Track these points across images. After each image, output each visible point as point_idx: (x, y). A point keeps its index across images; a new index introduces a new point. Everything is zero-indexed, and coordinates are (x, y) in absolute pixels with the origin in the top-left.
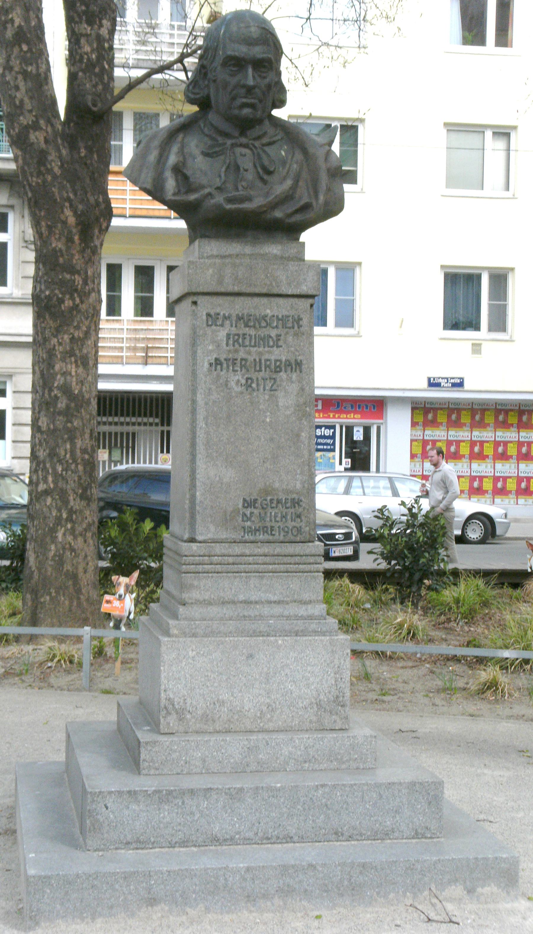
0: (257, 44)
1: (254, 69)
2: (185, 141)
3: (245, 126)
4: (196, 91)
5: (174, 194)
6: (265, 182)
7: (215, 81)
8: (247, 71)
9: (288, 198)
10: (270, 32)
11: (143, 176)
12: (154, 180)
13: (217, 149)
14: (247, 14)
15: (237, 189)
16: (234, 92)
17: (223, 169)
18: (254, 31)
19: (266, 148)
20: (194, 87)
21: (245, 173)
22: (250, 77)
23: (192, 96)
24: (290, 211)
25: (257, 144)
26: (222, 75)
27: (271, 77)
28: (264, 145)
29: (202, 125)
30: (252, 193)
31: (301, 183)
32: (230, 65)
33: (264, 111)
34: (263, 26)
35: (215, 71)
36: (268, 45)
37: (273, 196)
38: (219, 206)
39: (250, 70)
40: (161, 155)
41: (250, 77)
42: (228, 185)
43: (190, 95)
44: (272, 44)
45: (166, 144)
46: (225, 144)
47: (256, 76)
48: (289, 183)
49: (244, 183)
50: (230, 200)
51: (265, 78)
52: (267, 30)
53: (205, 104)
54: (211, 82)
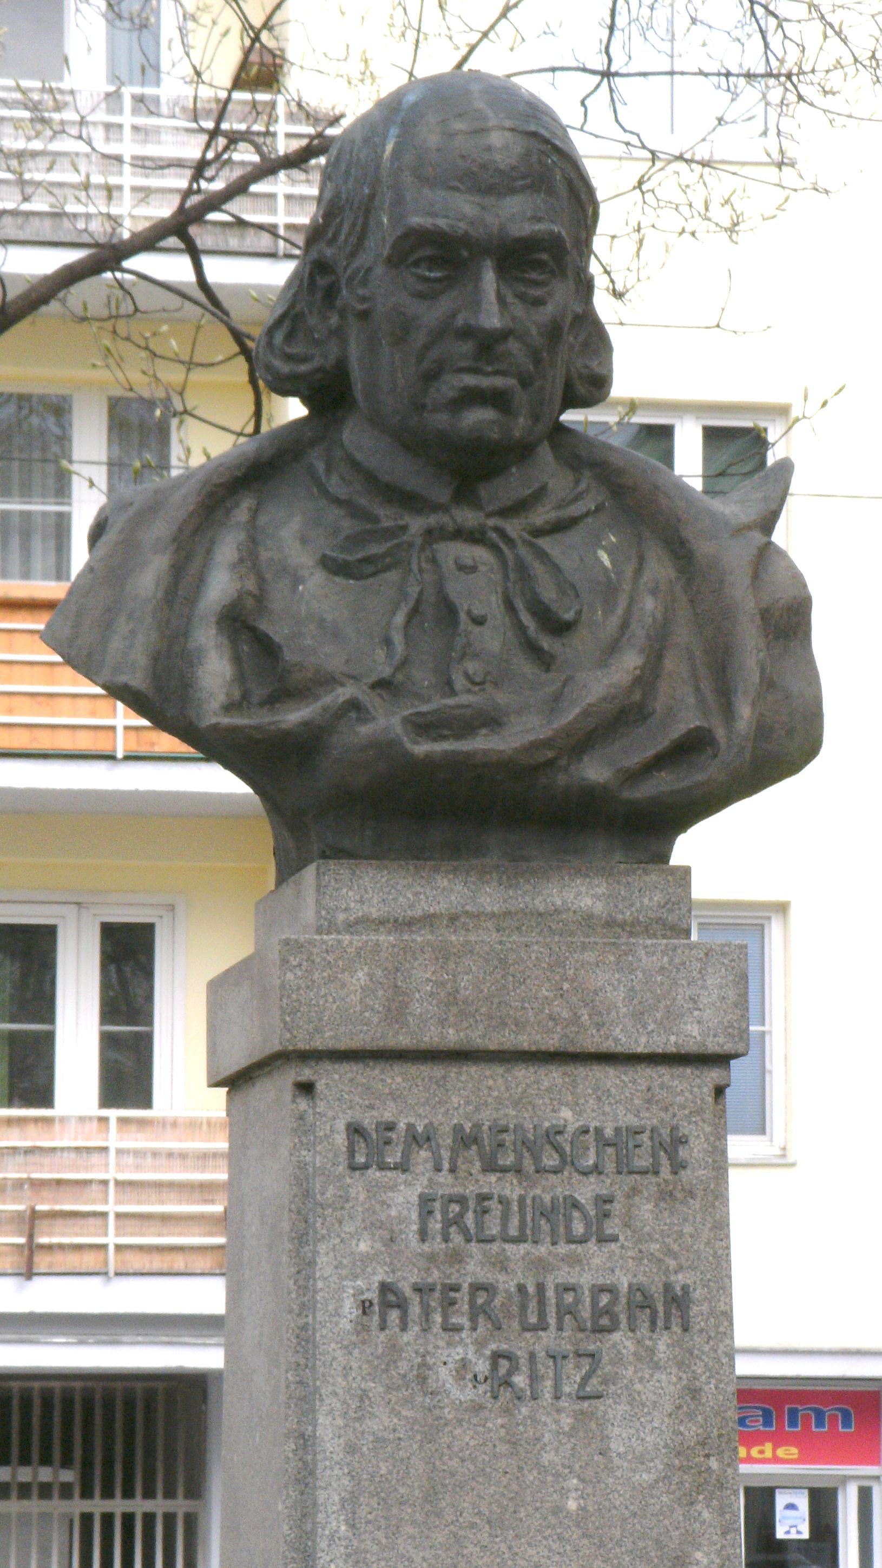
0: (512, 191)
1: (502, 271)
2: (263, 519)
3: (472, 467)
4: (297, 349)
5: (228, 708)
6: (544, 660)
7: (364, 315)
8: (478, 278)
9: (625, 715)
10: (556, 149)
11: (116, 644)
12: (156, 658)
13: (375, 549)
14: (475, 87)
15: (449, 688)
16: (434, 354)
17: (400, 619)
18: (502, 145)
19: (544, 543)
20: (290, 337)
21: (476, 630)
22: (489, 301)
23: (285, 368)
24: (635, 760)
25: (513, 527)
26: (388, 292)
27: (560, 295)
28: (538, 532)
29: (320, 466)
30: (501, 698)
31: (669, 664)
32: (416, 264)
33: (536, 418)
34: (532, 128)
35: (364, 283)
36: (551, 192)
37: (577, 710)
38: (385, 748)
39: (489, 278)
40: (177, 570)
41: (489, 301)
42: (417, 674)
43: (277, 363)
44: (562, 188)
45: (196, 532)
46: (404, 528)
47: (510, 299)
48: (630, 661)
49: (472, 666)
50: (425, 726)
51: (539, 302)
52: (547, 141)
53: (329, 396)
54: (352, 319)
